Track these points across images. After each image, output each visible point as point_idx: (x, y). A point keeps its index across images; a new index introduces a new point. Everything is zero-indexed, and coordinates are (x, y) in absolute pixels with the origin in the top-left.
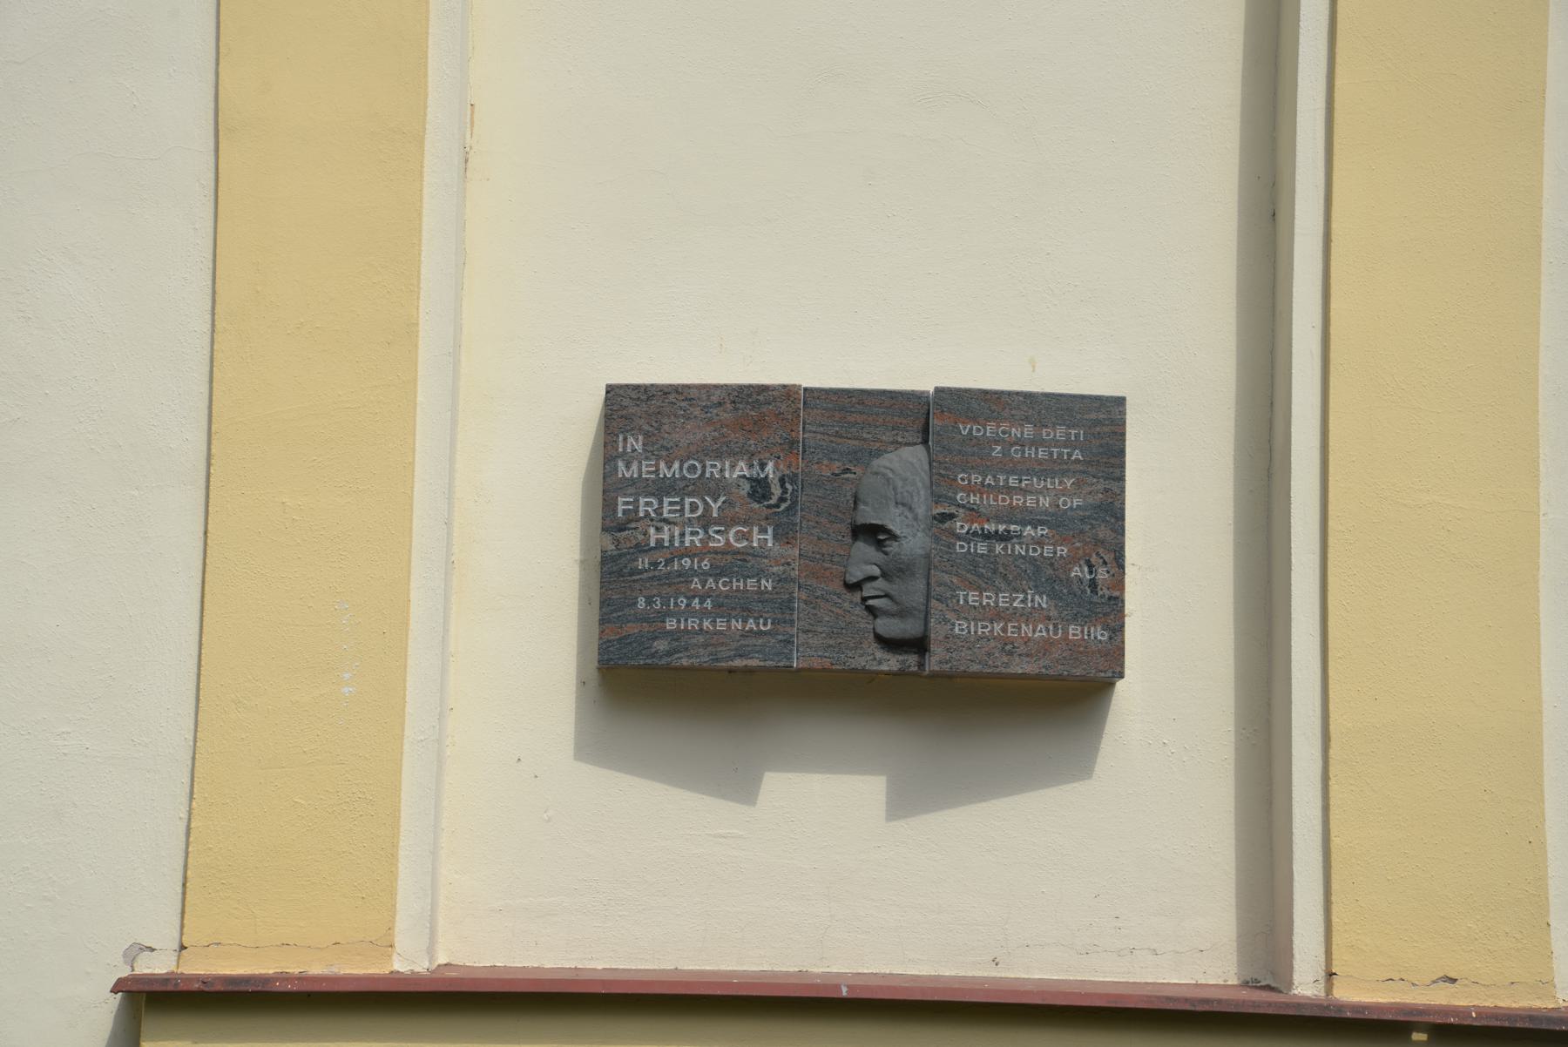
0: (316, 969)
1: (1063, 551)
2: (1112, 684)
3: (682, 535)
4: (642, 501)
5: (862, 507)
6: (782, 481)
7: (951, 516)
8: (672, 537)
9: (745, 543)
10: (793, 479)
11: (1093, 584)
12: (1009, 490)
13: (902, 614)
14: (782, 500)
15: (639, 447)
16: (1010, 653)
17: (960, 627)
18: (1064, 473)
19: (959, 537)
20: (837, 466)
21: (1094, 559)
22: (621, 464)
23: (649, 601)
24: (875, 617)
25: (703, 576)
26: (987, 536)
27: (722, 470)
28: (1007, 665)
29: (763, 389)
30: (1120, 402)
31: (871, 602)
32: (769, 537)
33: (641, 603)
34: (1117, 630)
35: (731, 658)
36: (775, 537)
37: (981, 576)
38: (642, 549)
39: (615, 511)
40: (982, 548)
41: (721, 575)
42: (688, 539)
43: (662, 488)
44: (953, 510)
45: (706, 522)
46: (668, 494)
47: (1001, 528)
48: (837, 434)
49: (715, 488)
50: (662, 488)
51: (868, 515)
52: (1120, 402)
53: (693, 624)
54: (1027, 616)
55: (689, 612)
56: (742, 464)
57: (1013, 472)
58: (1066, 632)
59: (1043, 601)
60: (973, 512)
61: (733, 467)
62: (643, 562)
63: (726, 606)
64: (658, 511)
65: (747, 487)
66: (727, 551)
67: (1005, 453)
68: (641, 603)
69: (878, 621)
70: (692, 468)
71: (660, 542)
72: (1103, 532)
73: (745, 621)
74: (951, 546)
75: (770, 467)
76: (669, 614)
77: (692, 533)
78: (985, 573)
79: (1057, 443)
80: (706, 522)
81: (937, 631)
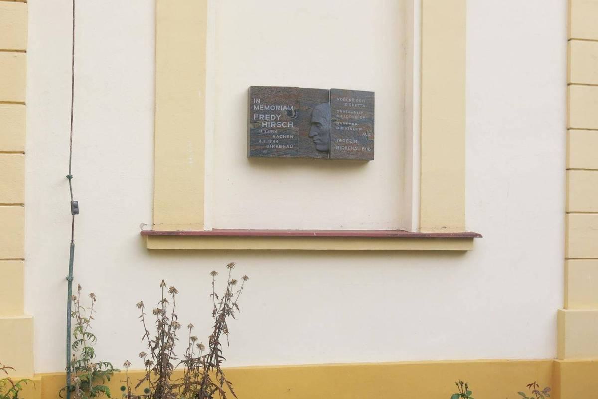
0: (186, 230)
1: (361, 129)
2: (369, 161)
3: (270, 124)
4: (260, 115)
5: (314, 118)
6: (295, 111)
7: (336, 120)
8: (268, 125)
9: (286, 126)
10: (298, 110)
11: (367, 137)
12: (349, 114)
13: (324, 144)
14: (295, 116)
15: (259, 102)
16: (349, 154)
17: (337, 147)
18: (361, 110)
19: (337, 126)
20: (307, 107)
21: (368, 131)
22: (255, 106)
23: (262, 140)
24: (317, 144)
25: (276, 135)
26: (344, 125)
27: (280, 108)
28: (348, 157)
29: (290, 88)
30: (373, 93)
31: (316, 141)
32: (292, 125)
33: (260, 141)
34: (373, 148)
35: (283, 155)
36: (293, 125)
37: (342, 135)
38: (260, 127)
39: (253, 118)
40: (342, 128)
41: (280, 134)
42: (272, 125)
43: (265, 112)
44: (335, 119)
45: (276, 121)
46: (266, 114)
47: (347, 123)
48: (307, 100)
49: (278, 112)
50: (265, 112)
51: (315, 119)
52: (373, 93)
53: (273, 146)
54: (352, 145)
55: (272, 143)
56: (285, 106)
57: (350, 110)
58: (361, 148)
59: (356, 141)
60: (341, 120)
61: (283, 107)
62: (260, 131)
63: (281, 142)
64: (264, 118)
65: (286, 113)
66: (282, 128)
67: (348, 105)
68: (260, 141)
69: (318, 146)
70: (272, 108)
71: (265, 126)
72: (370, 125)
73: (286, 146)
74: (335, 128)
75: (292, 107)
76: (267, 144)
77: (273, 124)
78: (343, 134)
79: (359, 103)
80: (276, 121)
81: (332, 149)
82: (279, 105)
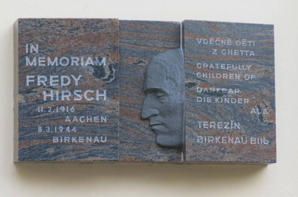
2: (266, 165)
3: (60, 95)
4: (39, 77)
6: (110, 67)
7: (194, 84)
8: (55, 96)
9: (92, 99)
10: (116, 66)
11: (261, 117)
12: (221, 71)
13: (171, 133)
14: (110, 77)
15: (36, 50)
16: (224, 152)
17: (200, 139)
18: (246, 62)
19: (198, 95)
20: (136, 60)
21: (261, 105)
22: (27, 59)
23: (44, 128)
26: (211, 94)
27: (80, 62)
28: (222, 157)
29: (99, 21)
30: (271, 27)
31: (155, 127)
32: (104, 95)
33: (40, 129)
34: (272, 139)
35: (87, 157)
36: (107, 95)
37: (209, 114)
38: (39, 102)
39: (25, 83)
40: (209, 100)
41: (81, 115)
43: (48, 71)
44: (195, 81)
45: (72, 88)
46: (52, 74)
47: (218, 90)
50: (48, 71)
51: (153, 84)
52: (271, 27)
53: (67, 139)
54: (231, 133)
55: (65, 133)
56: (89, 58)
57: (221, 62)
58: (249, 141)
59: (238, 126)
60: (204, 82)
61: (85, 60)
62: (40, 109)
63: (82, 130)
65: (92, 70)
66: (83, 102)
67: (219, 52)
68: (40, 129)
70: (64, 61)
71: (49, 98)
72: (265, 91)
73: (93, 138)
74: (194, 99)
75: (104, 60)
76: (55, 135)
77: (66, 94)
78: (210, 112)
80: (72, 88)
81: (189, 141)
82: (78, 55)
